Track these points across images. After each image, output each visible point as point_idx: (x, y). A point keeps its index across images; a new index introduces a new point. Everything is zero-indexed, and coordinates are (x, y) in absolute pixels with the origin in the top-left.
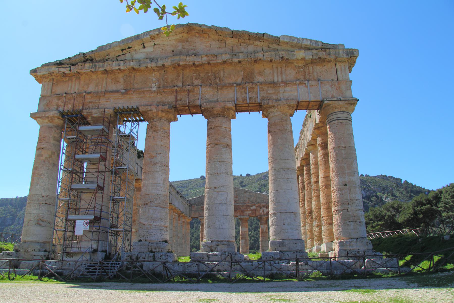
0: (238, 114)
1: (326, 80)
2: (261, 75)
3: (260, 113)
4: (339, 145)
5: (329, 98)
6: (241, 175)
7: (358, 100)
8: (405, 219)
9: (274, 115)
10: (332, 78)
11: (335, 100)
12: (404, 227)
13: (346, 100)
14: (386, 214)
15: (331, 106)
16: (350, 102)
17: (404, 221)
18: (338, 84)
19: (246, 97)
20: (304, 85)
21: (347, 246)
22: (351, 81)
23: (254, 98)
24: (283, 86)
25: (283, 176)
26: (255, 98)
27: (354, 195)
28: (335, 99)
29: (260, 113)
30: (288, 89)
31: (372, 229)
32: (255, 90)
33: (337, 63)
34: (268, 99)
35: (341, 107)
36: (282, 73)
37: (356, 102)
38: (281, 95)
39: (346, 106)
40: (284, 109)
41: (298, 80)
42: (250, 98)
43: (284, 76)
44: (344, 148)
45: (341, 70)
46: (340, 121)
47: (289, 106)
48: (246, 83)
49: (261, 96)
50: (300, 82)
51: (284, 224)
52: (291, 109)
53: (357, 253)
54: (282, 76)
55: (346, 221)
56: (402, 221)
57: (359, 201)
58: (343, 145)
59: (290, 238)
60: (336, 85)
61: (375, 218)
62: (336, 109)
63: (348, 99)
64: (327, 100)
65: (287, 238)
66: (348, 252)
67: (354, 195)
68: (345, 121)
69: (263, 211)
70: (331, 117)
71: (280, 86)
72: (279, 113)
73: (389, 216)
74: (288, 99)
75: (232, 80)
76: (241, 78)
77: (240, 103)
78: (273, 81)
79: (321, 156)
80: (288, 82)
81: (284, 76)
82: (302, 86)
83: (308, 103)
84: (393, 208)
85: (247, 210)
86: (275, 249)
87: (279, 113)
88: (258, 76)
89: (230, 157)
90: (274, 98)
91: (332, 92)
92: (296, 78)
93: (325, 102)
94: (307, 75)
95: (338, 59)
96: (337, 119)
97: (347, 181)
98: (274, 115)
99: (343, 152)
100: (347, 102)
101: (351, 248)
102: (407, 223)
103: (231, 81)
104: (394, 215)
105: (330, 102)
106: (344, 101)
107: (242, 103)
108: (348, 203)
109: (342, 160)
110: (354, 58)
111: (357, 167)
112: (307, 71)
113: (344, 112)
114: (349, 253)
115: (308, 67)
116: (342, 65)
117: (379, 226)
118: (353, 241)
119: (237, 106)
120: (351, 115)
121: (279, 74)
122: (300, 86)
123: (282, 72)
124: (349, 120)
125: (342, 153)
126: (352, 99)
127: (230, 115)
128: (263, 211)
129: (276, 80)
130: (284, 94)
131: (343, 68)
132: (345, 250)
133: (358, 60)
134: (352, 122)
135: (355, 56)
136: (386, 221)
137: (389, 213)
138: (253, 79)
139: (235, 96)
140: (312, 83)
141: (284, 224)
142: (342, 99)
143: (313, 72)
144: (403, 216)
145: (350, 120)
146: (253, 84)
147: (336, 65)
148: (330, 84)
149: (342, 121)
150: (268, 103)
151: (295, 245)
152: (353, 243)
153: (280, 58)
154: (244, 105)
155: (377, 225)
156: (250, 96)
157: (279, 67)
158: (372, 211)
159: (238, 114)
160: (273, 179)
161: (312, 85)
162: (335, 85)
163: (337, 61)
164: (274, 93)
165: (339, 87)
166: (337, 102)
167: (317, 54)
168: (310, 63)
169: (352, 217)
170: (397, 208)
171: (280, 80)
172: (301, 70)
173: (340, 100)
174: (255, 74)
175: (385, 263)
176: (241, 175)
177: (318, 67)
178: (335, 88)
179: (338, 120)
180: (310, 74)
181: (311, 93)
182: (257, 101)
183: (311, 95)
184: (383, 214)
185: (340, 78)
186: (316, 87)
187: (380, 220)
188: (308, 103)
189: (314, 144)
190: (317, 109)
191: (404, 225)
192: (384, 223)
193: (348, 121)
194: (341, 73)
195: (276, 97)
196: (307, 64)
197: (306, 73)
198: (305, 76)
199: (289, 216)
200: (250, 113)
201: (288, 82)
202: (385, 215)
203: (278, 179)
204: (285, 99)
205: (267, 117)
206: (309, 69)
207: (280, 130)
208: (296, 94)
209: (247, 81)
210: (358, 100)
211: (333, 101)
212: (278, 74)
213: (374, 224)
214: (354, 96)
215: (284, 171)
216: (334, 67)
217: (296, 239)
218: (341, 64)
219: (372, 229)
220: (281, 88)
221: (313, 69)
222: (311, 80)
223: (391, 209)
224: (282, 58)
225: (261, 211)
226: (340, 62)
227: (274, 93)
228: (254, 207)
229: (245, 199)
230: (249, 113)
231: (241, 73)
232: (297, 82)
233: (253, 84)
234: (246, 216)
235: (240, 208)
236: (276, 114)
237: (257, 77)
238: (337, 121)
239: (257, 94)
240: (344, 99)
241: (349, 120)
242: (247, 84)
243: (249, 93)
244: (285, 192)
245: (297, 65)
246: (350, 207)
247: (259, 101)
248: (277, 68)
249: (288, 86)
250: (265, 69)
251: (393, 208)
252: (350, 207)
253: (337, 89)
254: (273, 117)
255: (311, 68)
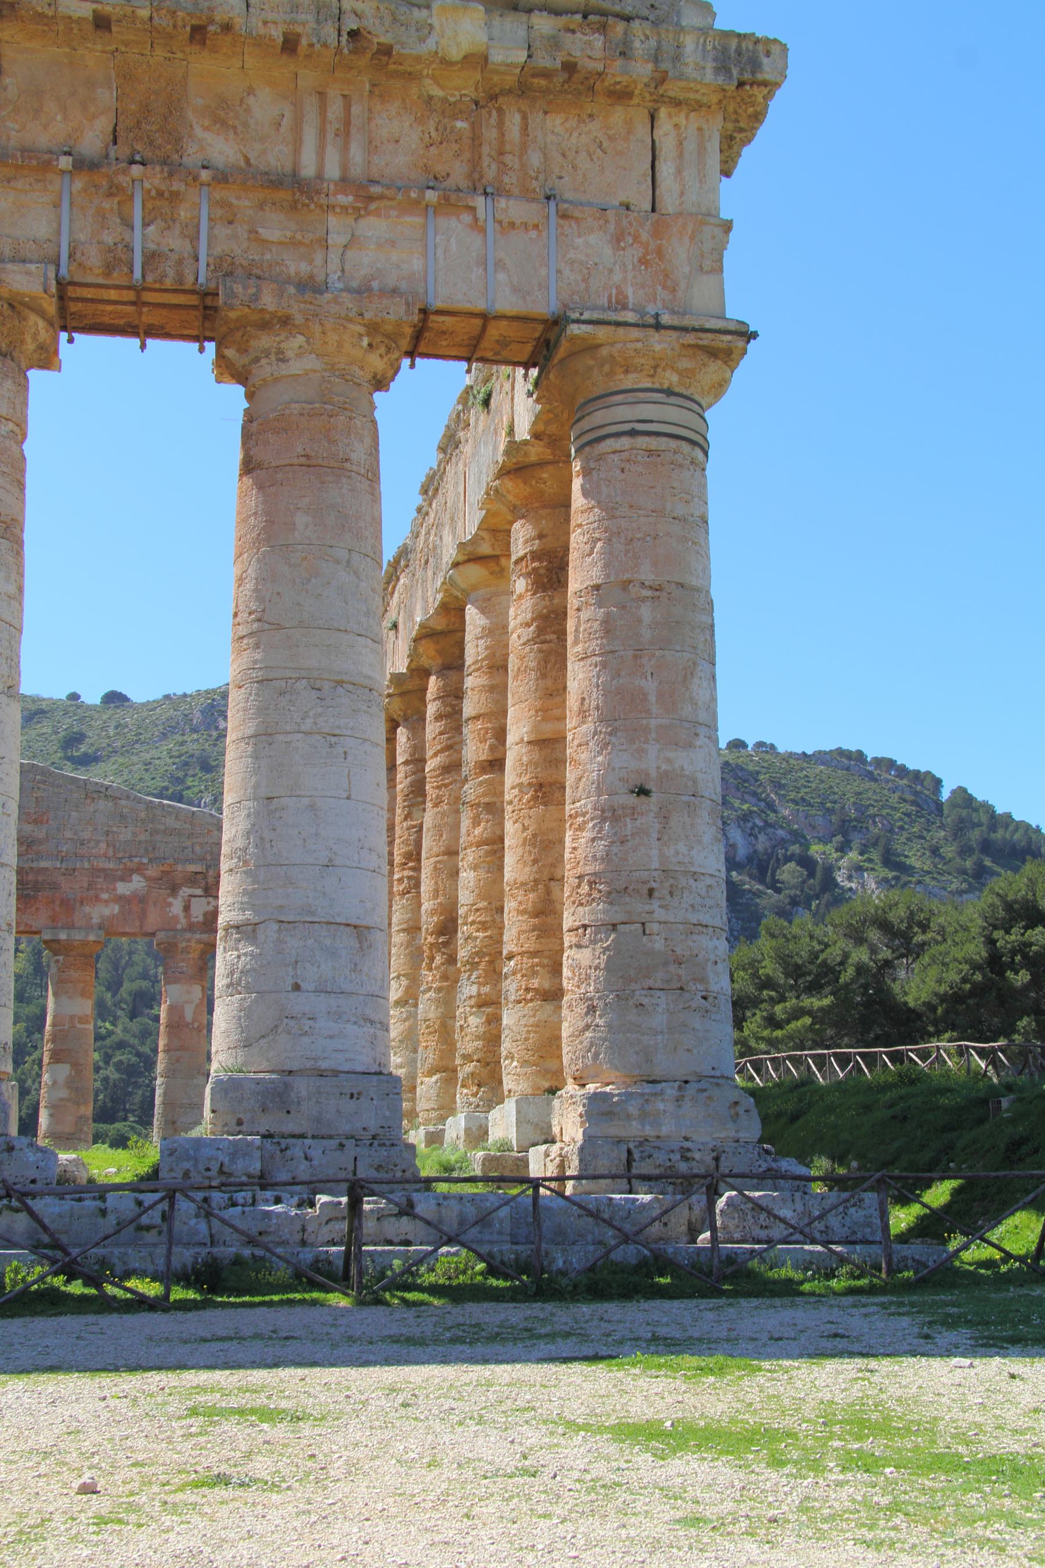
0: (71, 341)
1: (590, 204)
2: (224, 123)
3: (202, 350)
4: (627, 576)
5: (594, 308)
6: (74, 697)
7: (754, 335)
8: (943, 989)
9: (284, 370)
10: (623, 197)
11: (626, 324)
12: (931, 1029)
13: (684, 329)
14: (846, 956)
15: (604, 351)
16: (706, 339)
17: (935, 1001)
18: (657, 232)
19: (129, 248)
20: (467, 218)
21: (629, 1117)
22: (727, 226)
23: (174, 256)
24: (345, 209)
25: (309, 722)
26: (180, 262)
27: (682, 848)
28: (630, 317)
29: (202, 350)
30: (373, 227)
31: (766, 1033)
32: (183, 213)
33: (663, 113)
34: (254, 274)
35: (655, 367)
36: (345, 132)
37: (740, 343)
38: (334, 258)
39: (685, 364)
40: (340, 345)
41: (434, 181)
42: (151, 258)
43: (356, 153)
44: (648, 593)
45: (681, 156)
46: (642, 441)
47: (373, 328)
48: (132, 162)
49: (217, 251)
50: (446, 199)
51: (297, 987)
52: (382, 350)
53: (677, 1157)
54: (345, 148)
55: (633, 987)
56: (924, 997)
57: (709, 881)
58: (647, 574)
59: (324, 1065)
60: (645, 236)
61: (787, 975)
62: (627, 372)
63: (696, 324)
64: (586, 316)
65: (309, 1064)
66: (629, 1152)
67: (682, 848)
68: (673, 444)
69: (187, 908)
70: (599, 417)
71: (330, 207)
72: (311, 362)
73: (861, 969)
74: (370, 289)
75: (45, 127)
76: (103, 124)
77: (90, 279)
78: (295, 174)
79: (528, 625)
80: (376, 190)
81: (356, 153)
82: (453, 223)
83: (478, 322)
84: (885, 926)
85: (97, 898)
86: (240, 1123)
87: (311, 362)
88: (206, 129)
89: (12, 589)
90: (292, 271)
91: (617, 277)
92: (426, 169)
93: (575, 329)
94: (486, 161)
95: (672, 89)
96: (627, 427)
97: (654, 774)
98: (284, 370)
99: (646, 612)
100: (690, 339)
101: (649, 1131)
102: (947, 1012)
103: (43, 139)
104: (887, 964)
105: (602, 333)
106: (674, 334)
107: (101, 281)
108: (651, 892)
109: (635, 657)
110: (759, 93)
111: (714, 699)
112: (490, 134)
113: (669, 392)
114: (636, 1156)
115: (500, 111)
116: (691, 123)
117: (807, 1020)
118: (662, 1092)
119: (71, 291)
120: (707, 415)
121: (330, 136)
122: (443, 222)
123: (347, 123)
124: (693, 443)
125: (640, 621)
126: (718, 324)
127: (23, 342)
128: (187, 908)
129: (308, 170)
130: (350, 254)
131: (691, 146)
132: (619, 1141)
133: (779, 106)
134: (706, 454)
135: (765, 84)
136: (842, 994)
137: (861, 955)
138: (177, 141)
139: (58, 232)
140: (515, 209)
141: (297, 987)
142: (666, 319)
143: (524, 148)
144: (933, 972)
145: (701, 440)
146: (171, 175)
147: (653, 118)
148: (612, 227)
149: (653, 443)
150: (256, 297)
151: (350, 1106)
152: (661, 1106)
153: (344, 38)
154: (113, 295)
155: (797, 1013)
156: (152, 246)
157: (334, 94)
158: (773, 936)
159: (71, 341)
160: (250, 732)
161: (512, 225)
162: (636, 238)
163: (661, 99)
164: (294, 243)
165: (660, 252)
166: (635, 333)
167: (554, 43)
168: (510, 91)
169: (666, 964)
170: (903, 926)
171: (333, 171)
172: (459, 124)
173: (658, 326)
174: (190, 115)
175: (821, 1217)
176: (74, 697)
177: (556, 122)
178: (636, 252)
179: (633, 433)
180: (508, 159)
181: (499, 264)
182: (190, 279)
183: (502, 276)
184: (833, 954)
185: (669, 202)
186: (534, 234)
187: (814, 988)
188: (478, 322)
189: (496, 558)
190: (527, 366)
191: (935, 1022)
192: (831, 1007)
193: (685, 447)
194: (679, 171)
195: (304, 268)
196: (494, 97)
197: (486, 150)
198: (475, 163)
199: (328, 942)
200: (143, 347)
201: (376, 190)
202: (842, 963)
203: (281, 737)
204: (355, 284)
205: (241, 377)
206: (500, 125)
207: (309, 463)
208: (417, 264)
209: (139, 147)
210: (754, 335)
211: (618, 324)
212: (322, 133)
213: (778, 1009)
214: (735, 311)
215: (314, 694)
216: (642, 130)
217: (360, 1069)
218: (681, 119)
219: (766, 1033)
220: (333, 221)
221: (525, 128)
222: (508, 195)
223: (874, 935)
224: (354, 34)
225: (177, 907)
226: (677, 103)
227: (294, 243)
228: (137, 883)
229: (86, 835)
230: (137, 342)
231: (106, 96)
232: (431, 196)
233: (171, 175)
234: (89, 928)
235: (55, 886)
236: (295, 367)
237: (198, 131)
238: (625, 442)
239: (195, 239)
240: (676, 322)
241: (693, 443)
242: (136, 170)
243: (146, 225)
244: (312, 807)
245: (437, 92)
246: (660, 914)
247: (202, 280)
248: (322, 95)
249: (377, 213)
250: (251, 91)
251: (885, 926)
252: (660, 914)
253: (643, 261)
254: (277, 380)
255: (514, 121)
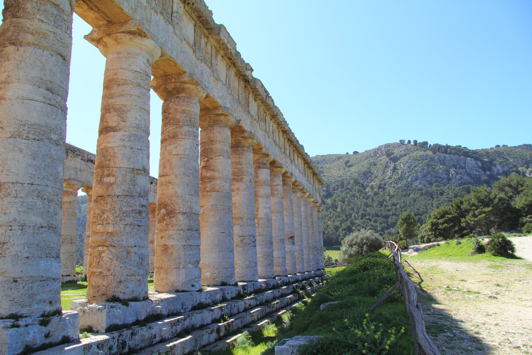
6: (347, 153)
8: (527, 203)
12: (524, 215)
14: (496, 195)
17: (525, 206)
31: (472, 219)
56: (521, 205)
61: (479, 203)
73: (500, 199)
84: (510, 186)
102: (528, 209)
104: (511, 197)
117: (484, 215)
136: (496, 207)
137: (502, 195)
144: (524, 198)
155: (480, 214)
158: (474, 192)
170: (515, 186)
176: (347, 153)
184: (492, 196)
187: (487, 205)
191: (525, 212)
192: (491, 210)
202: (495, 198)
213: (476, 212)
219: (472, 219)
223: (507, 188)
251: (510, 186)
